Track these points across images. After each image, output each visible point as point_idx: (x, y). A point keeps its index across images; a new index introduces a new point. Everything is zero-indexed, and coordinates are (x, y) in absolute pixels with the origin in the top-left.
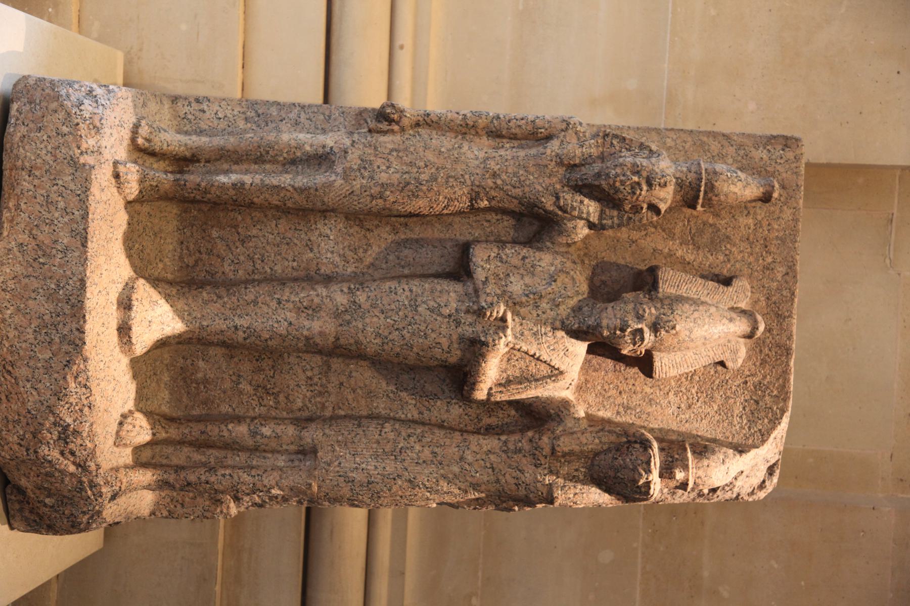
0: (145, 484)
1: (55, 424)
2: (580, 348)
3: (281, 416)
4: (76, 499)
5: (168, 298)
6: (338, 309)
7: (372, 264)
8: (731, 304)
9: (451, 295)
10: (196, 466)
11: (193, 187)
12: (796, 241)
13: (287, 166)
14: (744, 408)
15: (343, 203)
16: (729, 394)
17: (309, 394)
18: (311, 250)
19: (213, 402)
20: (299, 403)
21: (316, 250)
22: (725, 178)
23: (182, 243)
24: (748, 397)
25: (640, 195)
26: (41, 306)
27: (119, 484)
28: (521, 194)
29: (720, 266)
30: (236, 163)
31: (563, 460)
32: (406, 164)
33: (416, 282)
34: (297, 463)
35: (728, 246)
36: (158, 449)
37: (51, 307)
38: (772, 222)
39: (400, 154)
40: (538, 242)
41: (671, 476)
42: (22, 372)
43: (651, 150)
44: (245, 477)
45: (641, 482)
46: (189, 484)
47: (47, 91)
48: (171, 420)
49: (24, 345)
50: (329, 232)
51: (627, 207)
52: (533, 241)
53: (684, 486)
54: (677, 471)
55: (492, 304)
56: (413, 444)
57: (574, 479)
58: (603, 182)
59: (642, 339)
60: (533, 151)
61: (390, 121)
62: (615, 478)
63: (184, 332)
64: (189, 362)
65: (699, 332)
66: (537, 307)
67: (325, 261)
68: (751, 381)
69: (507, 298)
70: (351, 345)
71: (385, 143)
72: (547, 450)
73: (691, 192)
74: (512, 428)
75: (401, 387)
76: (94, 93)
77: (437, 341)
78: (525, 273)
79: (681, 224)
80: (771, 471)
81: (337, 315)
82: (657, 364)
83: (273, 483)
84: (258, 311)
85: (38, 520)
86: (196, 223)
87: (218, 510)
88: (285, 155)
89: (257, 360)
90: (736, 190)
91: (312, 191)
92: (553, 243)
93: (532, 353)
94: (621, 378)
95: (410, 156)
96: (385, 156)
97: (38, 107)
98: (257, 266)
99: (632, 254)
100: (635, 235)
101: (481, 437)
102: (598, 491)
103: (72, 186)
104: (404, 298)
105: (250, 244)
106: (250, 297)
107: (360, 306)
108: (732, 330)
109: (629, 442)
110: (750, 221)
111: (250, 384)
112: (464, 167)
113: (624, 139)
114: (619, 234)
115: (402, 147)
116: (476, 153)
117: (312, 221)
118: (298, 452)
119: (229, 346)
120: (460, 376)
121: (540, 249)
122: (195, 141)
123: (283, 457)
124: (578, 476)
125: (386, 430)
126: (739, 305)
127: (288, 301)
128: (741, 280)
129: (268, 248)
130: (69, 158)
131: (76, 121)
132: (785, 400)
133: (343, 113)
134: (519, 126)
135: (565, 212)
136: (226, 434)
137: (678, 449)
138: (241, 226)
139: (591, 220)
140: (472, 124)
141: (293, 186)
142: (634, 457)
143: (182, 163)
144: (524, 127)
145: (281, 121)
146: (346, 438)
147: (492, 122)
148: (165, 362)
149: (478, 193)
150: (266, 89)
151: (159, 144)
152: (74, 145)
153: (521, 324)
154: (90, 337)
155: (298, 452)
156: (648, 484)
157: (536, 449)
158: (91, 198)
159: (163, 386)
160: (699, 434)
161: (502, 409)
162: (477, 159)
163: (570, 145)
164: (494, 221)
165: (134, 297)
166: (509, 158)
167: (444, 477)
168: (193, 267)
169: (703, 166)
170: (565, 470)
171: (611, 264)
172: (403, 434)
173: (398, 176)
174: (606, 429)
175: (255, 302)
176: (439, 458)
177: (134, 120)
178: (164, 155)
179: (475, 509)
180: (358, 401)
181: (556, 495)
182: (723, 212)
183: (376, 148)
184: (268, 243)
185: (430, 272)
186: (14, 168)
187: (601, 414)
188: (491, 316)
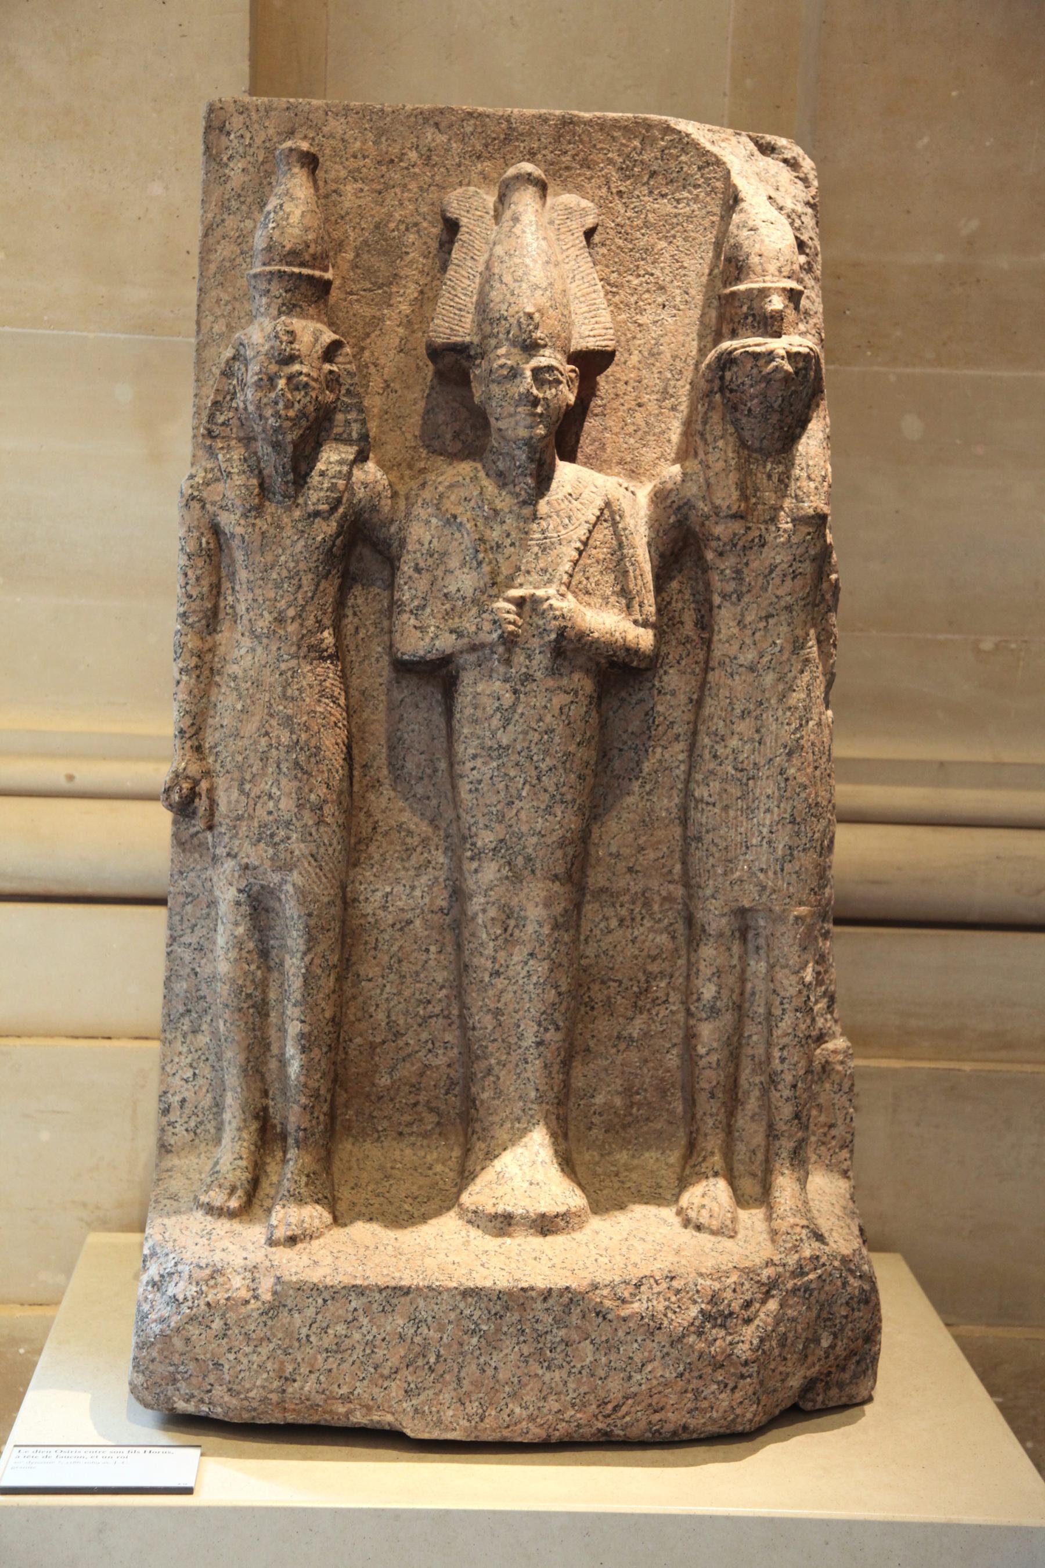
0: (797, 1187)
1: (700, 1334)
2: (565, 472)
3: (684, 969)
4: (823, 1297)
5: (491, 1156)
6: (507, 878)
7: (431, 821)
8: (489, 219)
9: (481, 691)
10: (767, 1105)
11: (308, 1117)
12: (382, 110)
13: (272, 964)
14: (663, 196)
15: (331, 871)
16: (639, 222)
17: (647, 923)
18: (409, 922)
19: (662, 1080)
20: (663, 939)
21: (409, 915)
22: (277, 232)
23: (401, 1134)
24: (645, 190)
26: (507, 1360)
27: (798, 1230)
28: (310, 576)
29: (425, 238)
30: (267, 1046)
31: (754, 500)
32: (265, 767)
33: (460, 748)
34: (761, 941)
35: (392, 225)
36: (739, 1168)
37: (508, 1343)
38: (350, 151)
39: (248, 777)
40: (390, 546)
41: (778, 317)
42: (615, 1386)
43: (234, 358)
44: (785, 1024)
45: (788, 367)
46: (797, 1116)
47: (155, 1354)
48: (691, 1146)
49: (572, 1386)
50: (379, 894)
51: (330, 397)
52: (389, 556)
53: (793, 296)
54: (770, 308)
55: (495, 622)
56: (729, 750)
58: (289, 438)
59: (550, 369)
60: (239, 556)
61: (193, 795)
62: (782, 412)
63: (548, 1128)
64: (596, 1120)
65: (537, 274)
66: (498, 546)
67: (427, 900)
68: (617, 185)
69: (485, 597)
70: (565, 855)
71: (229, 802)
72: (737, 527)
73: (303, 289)
74: (701, 587)
75: (634, 771)
76: (157, 1278)
77: (557, 712)
78: (442, 568)
79: (356, 306)
80: (767, 150)
81: (516, 878)
82: (591, 344)
83: (794, 979)
84: (511, 1007)
85: (857, 1358)
86: (367, 1112)
87: (839, 1068)
88: (253, 967)
89: (593, 1008)
90: (298, 213)
91: (312, 923)
92: (392, 521)
93: (575, 554)
94: (615, 404)
95: (251, 761)
96: (251, 803)
97: (181, 1368)
98: (437, 1010)
99: (408, 388)
100: (376, 383)
101: (716, 638)
102: (804, 440)
103: (310, 1312)
104: (485, 769)
105: (401, 1022)
106: (488, 1021)
107: (501, 841)
108: (533, 219)
109: (721, 390)
110: (350, 188)
111: (632, 1019)
112: (267, 671)
113: (215, 403)
114: (376, 410)
115: (236, 775)
116: (243, 651)
117: (362, 921)
118: (744, 939)
119: (570, 1054)
120: (616, 673)
121: (403, 543)
122: (232, 1114)
123: (752, 963)
125: (706, 794)
126: (491, 205)
127: (494, 960)
128: (449, 203)
129: (407, 993)
130: (264, 1318)
131: (203, 1307)
132: (649, 126)
133: (181, 873)
134: (198, 579)
135: (339, 501)
136: (714, 1058)
137: (732, 306)
138: (371, 1038)
139: (352, 457)
140: (195, 660)
141: (305, 954)
142: (748, 382)
143: (269, 1136)
144: (199, 572)
145: (196, 974)
146: (719, 860)
147: (191, 626)
148: (597, 1159)
149: (311, 648)
150: (143, 998)
151: (238, 1173)
152: (243, 1310)
153: (528, 572)
154: (557, 1280)
155: (744, 939)
156: (792, 356)
157: (735, 545)
158: (329, 1282)
159: (636, 1162)
160: (707, 271)
161: (669, 603)
162: (253, 650)
163: (228, 493)
164: (356, 620)
165: (490, 1210)
166: (250, 596)
167: (783, 697)
168: (439, 1115)
169: (258, 269)
171: (425, 423)
172: (712, 765)
173: (284, 781)
174: (699, 427)
175: (497, 1013)
176: (752, 707)
177: (199, 1214)
178: (256, 1164)
179: (835, 646)
180: (659, 842)
181: (811, 511)
182: (335, 235)
183: (239, 818)
184: (399, 993)
185: (443, 725)
186: (281, 1405)
187: (675, 437)
188: (514, 623)
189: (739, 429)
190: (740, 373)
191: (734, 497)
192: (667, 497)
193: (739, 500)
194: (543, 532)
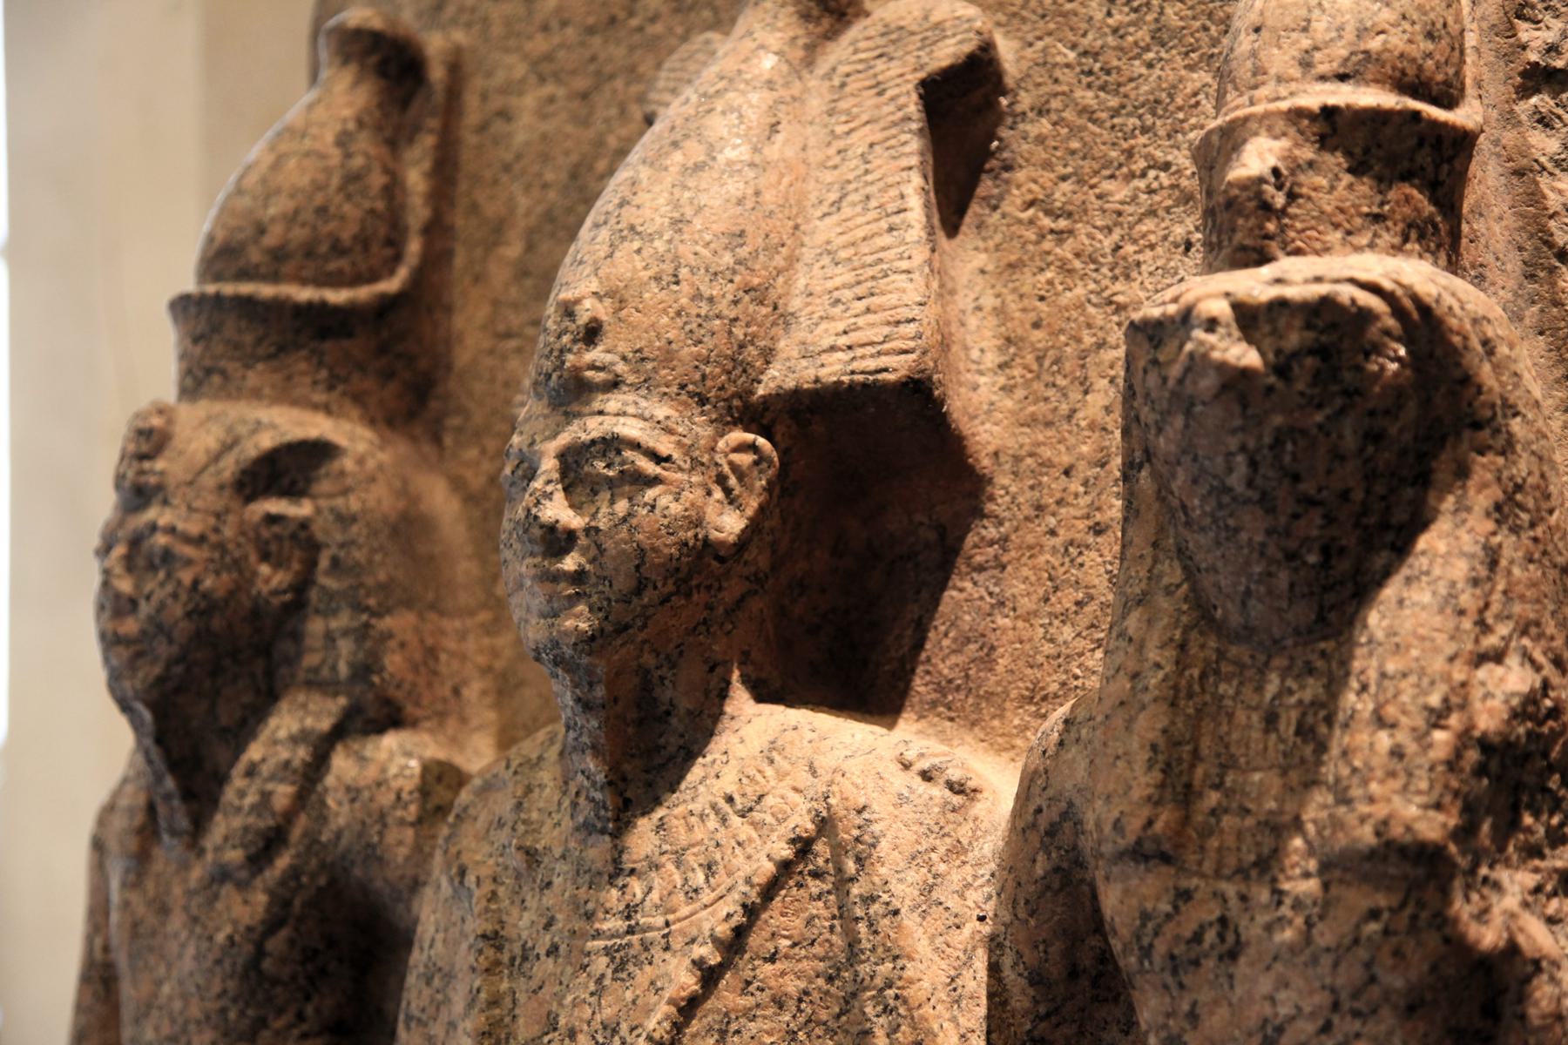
16: (1143, 35)
25: (171, 530)
31: (1213, 798)
45: (1247, 356)
57: (1315, 728)
62: (1266, 502)
93: (688, 982)
124: (1304, 708)
139: (325, 725)
191: (1136, 794)
193: (1155, 802)
194: (630, 911)
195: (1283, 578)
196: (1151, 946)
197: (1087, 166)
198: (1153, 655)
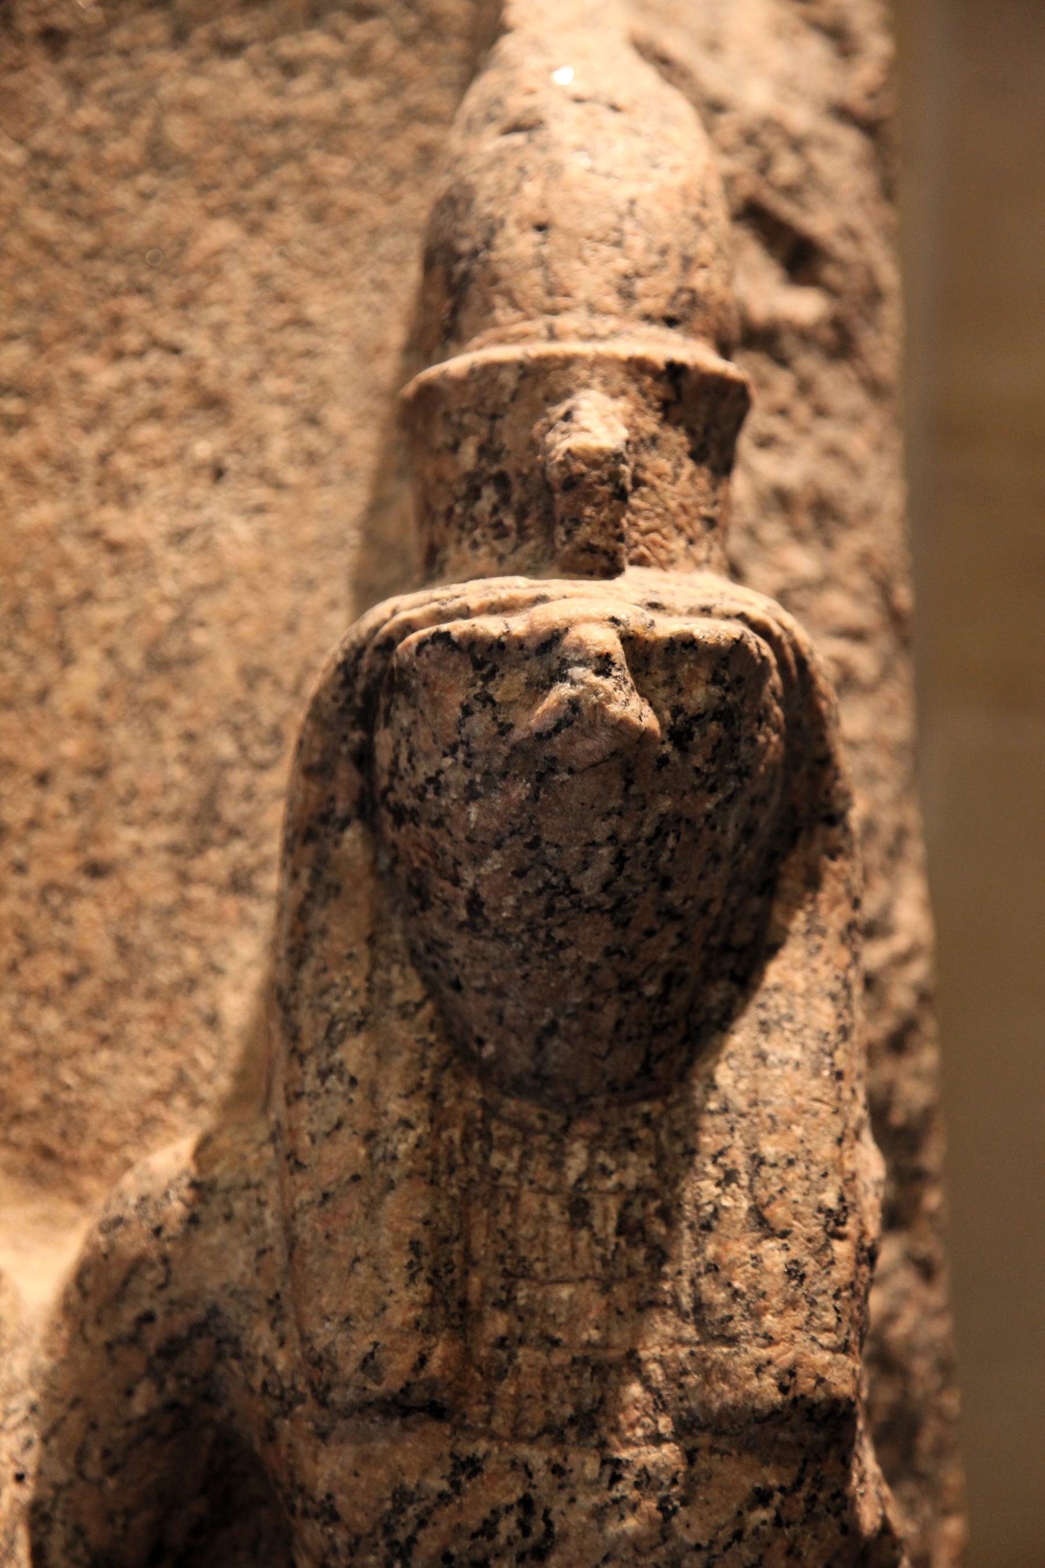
14: (232, 49)
16: (124, 148)
31: (499, 1324)
41: (609, 483)
45: (634, 709)
54: (562, 443)
57: (650, 1226)
62: (619, 912)
72: (414, 1457)
102: (742, 1037)
109: (367, 807)
124: (628, 1197)
142: (456, 776)
156: (650, 659)
170: (574, 1304)
181: (766, 1389)
187: (237, 1003)
189: (441, 984)
190: (422, 738)
191: (397, 1317)
192: (121, 1294)
193: (423, 1329)
195: (610, 1013)
196: (412, 1540)
197: (49, 327)
198: (395, 1107)
